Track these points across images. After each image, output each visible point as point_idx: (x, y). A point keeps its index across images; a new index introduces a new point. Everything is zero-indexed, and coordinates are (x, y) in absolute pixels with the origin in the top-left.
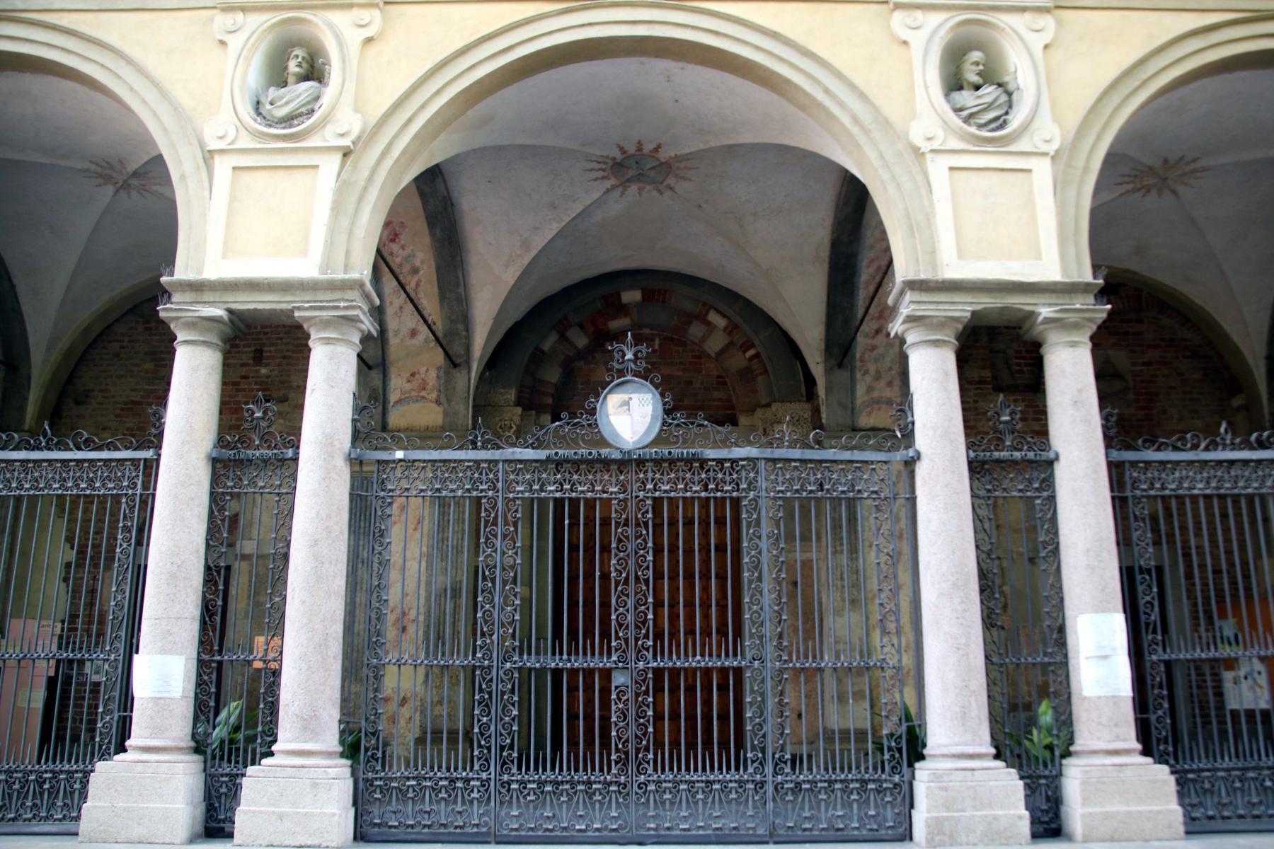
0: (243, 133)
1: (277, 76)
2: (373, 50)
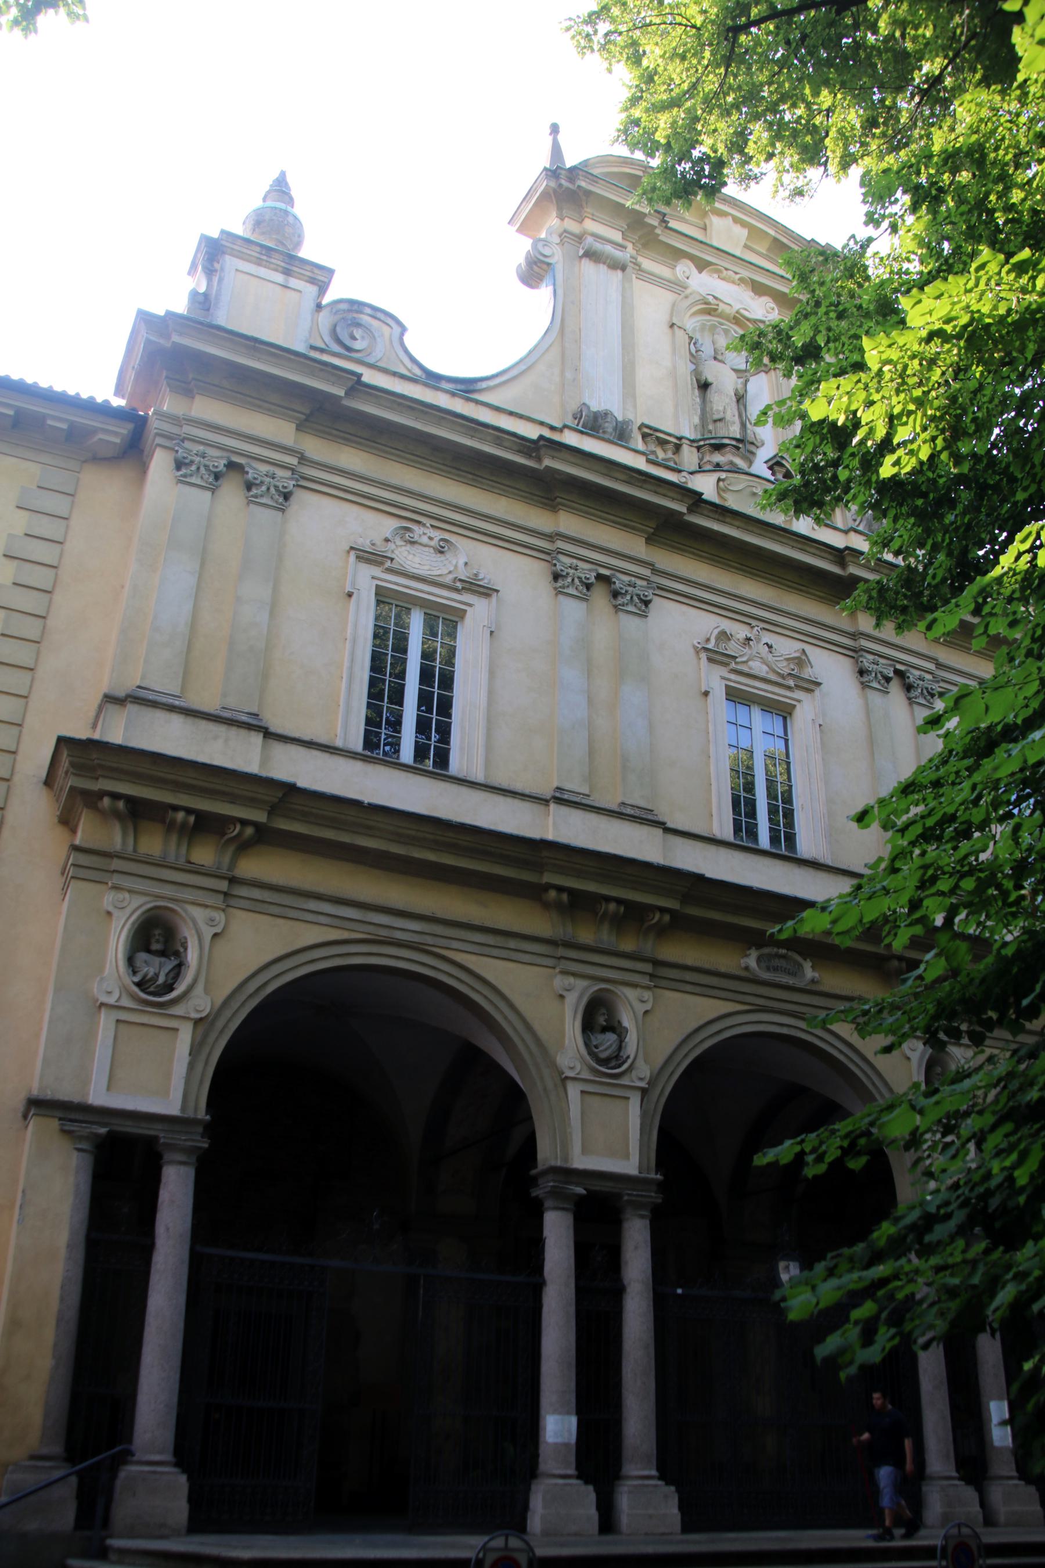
0: (585, 1067)
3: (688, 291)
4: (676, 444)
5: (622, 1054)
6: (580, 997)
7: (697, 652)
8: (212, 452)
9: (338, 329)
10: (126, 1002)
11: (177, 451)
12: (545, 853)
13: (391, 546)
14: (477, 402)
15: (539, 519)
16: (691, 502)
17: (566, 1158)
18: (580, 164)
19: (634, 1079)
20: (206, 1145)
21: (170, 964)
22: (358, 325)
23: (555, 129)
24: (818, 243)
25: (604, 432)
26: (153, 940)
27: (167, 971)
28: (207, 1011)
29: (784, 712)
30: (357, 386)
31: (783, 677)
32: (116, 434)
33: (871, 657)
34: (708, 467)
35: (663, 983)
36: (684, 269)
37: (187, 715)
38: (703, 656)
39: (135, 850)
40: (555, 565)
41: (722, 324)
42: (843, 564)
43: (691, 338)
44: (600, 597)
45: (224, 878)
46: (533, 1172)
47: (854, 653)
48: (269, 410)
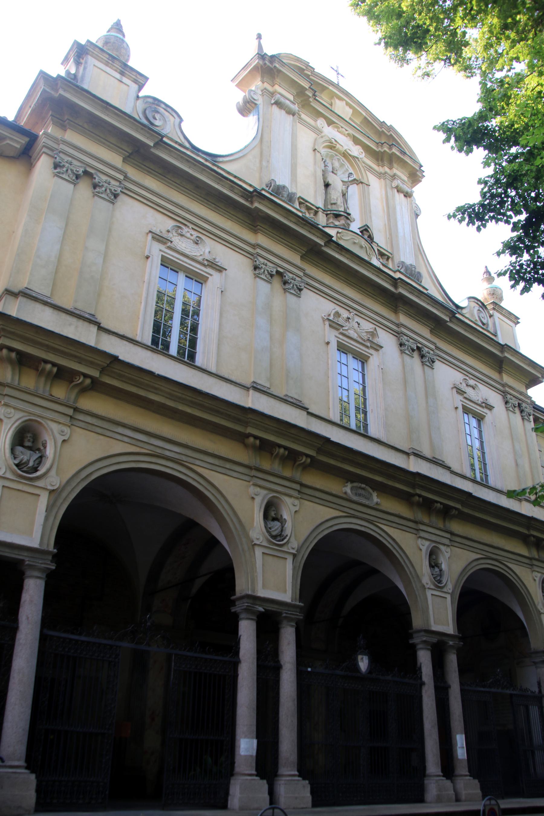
3: (323, 134)
4: (315, 211)
5: (283, 533)
6: (263, 499)
7: (324, 321)
8: (75, 162)
9: (147, 112)
10: (9, 475)
11: (56, 158)
12: (250, 416)
13: (170, 235)
14: (218, 167)
16: (326, 240)
17: (253, 590)
18: (277, 54)
19: (290, 548)
20: (54, 568)
21: (36, 455)
22: (158, 112)
23: (259, 37)
24: (386, 124)
25: (282, 196)
26: (26, 440)
27: (34, 459)
28: (58, 485)
29: (363, 360)
30: (160, 142)
31: (364, 341)
32: (18, 142)
33: (406, 337)
34: (332, 225)
35: (305, 497)
36: (321, 123)
37: (54, 308)
38: (327, 323)
39: (19, 384)
40: (256, 261)
41: (336, 155)
42: (396, 287)
43: (323, 159)
44: (277, 283)
45: (70, 407)
46: (233, 598)
47: (398, 334)
48: (109, 146)
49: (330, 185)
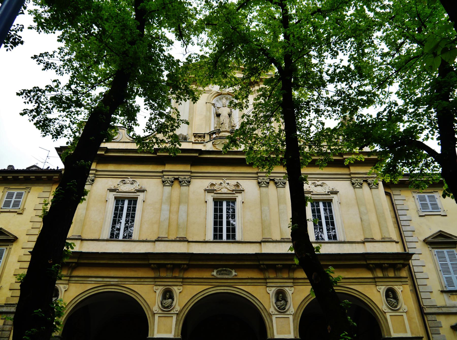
0: (160, 310)
1: (164, 298)
2: (181, 294)
15: (160, 169)
44: (176, 184)
49: (220, 114)
